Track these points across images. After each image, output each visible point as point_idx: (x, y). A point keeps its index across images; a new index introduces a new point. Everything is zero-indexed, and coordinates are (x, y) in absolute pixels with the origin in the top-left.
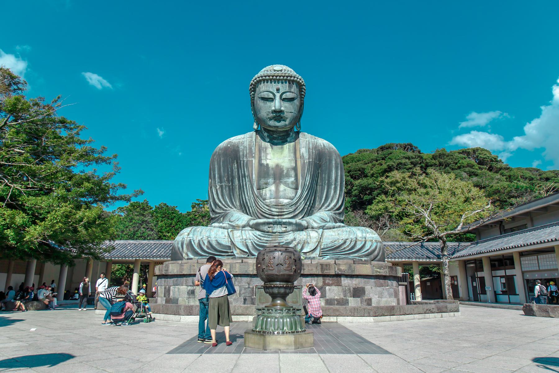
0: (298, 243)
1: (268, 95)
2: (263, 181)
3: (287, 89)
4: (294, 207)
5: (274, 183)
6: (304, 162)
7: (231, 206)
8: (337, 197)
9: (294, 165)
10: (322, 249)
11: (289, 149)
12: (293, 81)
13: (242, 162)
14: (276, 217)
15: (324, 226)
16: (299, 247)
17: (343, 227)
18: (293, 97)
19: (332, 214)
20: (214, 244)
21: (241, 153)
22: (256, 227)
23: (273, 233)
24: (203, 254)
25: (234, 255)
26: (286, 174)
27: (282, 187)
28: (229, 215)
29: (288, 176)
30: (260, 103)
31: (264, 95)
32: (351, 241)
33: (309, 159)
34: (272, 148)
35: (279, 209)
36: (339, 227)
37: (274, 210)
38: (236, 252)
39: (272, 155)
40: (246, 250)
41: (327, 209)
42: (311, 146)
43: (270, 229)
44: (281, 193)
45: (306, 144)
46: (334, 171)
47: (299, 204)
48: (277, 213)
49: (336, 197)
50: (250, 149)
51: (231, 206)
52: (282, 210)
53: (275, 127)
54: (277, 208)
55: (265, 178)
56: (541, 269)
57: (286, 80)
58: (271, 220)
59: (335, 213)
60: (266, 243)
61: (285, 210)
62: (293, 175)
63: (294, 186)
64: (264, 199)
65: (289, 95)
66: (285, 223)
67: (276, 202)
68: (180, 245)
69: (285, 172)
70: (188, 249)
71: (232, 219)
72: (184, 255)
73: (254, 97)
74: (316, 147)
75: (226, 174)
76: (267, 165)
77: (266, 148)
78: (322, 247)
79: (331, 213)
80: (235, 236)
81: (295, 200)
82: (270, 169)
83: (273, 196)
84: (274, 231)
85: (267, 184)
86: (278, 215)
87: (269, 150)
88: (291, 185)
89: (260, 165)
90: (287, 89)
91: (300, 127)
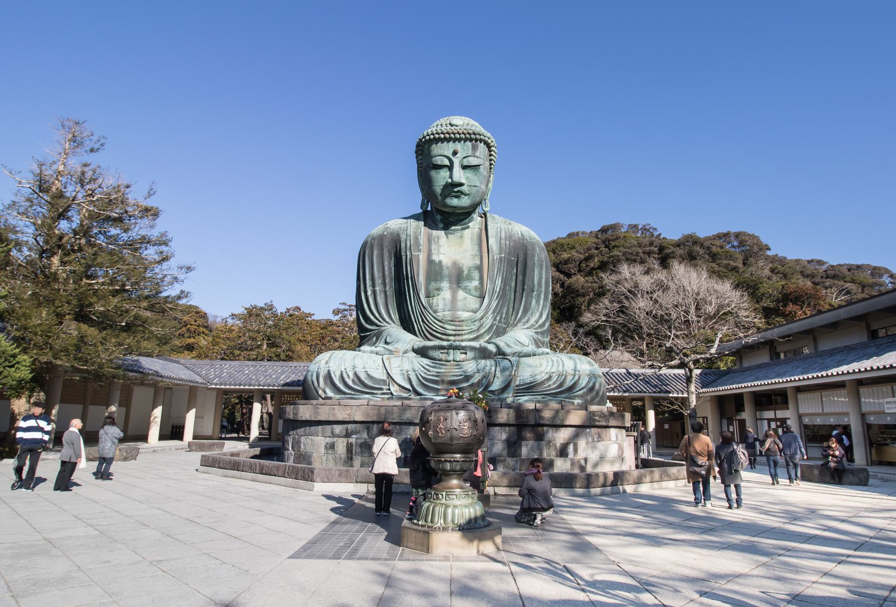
1: (442, 161)
2: (433, 285)
3: (470, 153)
4: (477, 324)
5: (450, 288)
6: (493, 259)
7: (387, 319)
9: (479, 263)
10: (517, 386)
12: (481, 141)
13: (404, 258)
14: (452, 338)
19: (533, 334)
20: (363, 377)
21: (403, 245)
22: (422, 352)
23: (447, 361)
24: (347, 391)
25: (392, 394)
27: (461, 294)
28: (385, 334)
29: (470, 278)
30: (433, 173)
33: (500, 253)
36: (543, 354)
38: (394, 389)
40: (409, 387)
43: (443, 357)
45: (497, 232)
48: (454, 333)
49: (540, 311)
50: (416, 238)
51: (387, 319)
53: (452, 207)
55: (436, 280)
56: (825, 411)
58: (445, 343)
60: (437, 376)
61: (465, 328)
62: (477, 278)
63: (477, 294)
64: (435, 312)
65: (473, 161)
66: (463, 348)
67: (452, 315)
68: (315, 379)
69: (466, 272)
70: (325, 383)
71: (388, 340)
72: (320, 392)
74: (510, 237)
75: (381, 274)
76: (440, 262)
78: (517, 383)
79: (531, 332)
80: (393, 366)
81: (479, 314)
83: (448, 308)
85: (439, 289)
86: (455, 335)
89: (430, 262)
90: (470, 153)
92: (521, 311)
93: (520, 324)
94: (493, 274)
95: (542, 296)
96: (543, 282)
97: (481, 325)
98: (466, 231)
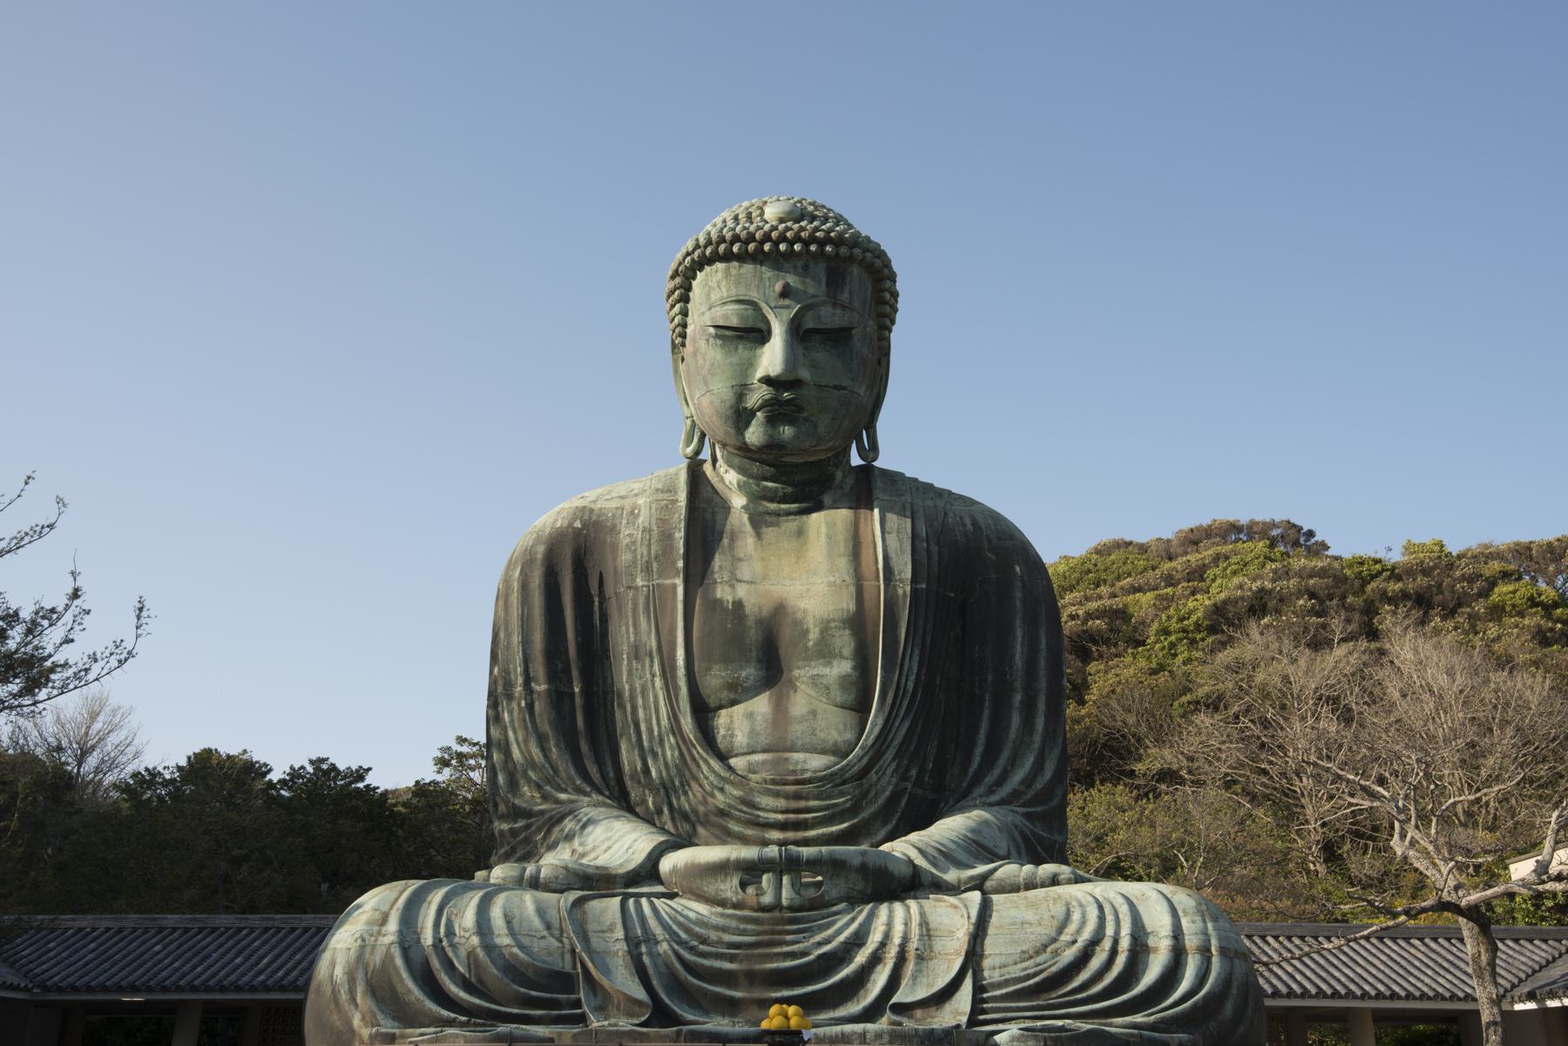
0: (876, 959)
8: (1036, 745)
9: (852, 607)
11: (829, 537)
15: (985, 877)
16: (880, 978)
17: (1069, 882)
18: (845, 324)
19: (1019, 820)
25: (582, 1019)
26: (817, 644)
27: (799, 704)
29: (825, 652)
31: (726, 317)
32: (1114, 952)
34: (758, 535)
35: (787, 797)
36: (1054, 881)
37: (765, 801)
39: (758, 567)
41: (994, 798)
42: (922, 530)
44: (797, 731)
46: (1019, 633)
47: (873, 776)
48: (780, 817)
50: (666, 537)
52: (802, 804)
54: (777, 795)
55: (726, 660)
57: (814, 255)
59: (1025, 815)
60: (731, 958)
61: (812, 803)
63: (850, 698)
65: (830, 317)
68: (339, 972)
73: (684, 325)
76: (738, 605)
77: (734, 537)
79: (1012, 816)
82: (751, 622)
83: (764, 740)
84: (767, 899)
86: (783, 826)
87: (748, 543)
88: (838, 695)
91: (874, 447)
92: (979, 750)
93: (979, 790)
94: (897, 641)
95: (1041, 706)
96: (1042, 664)
97: (864, 795)
98: (814, 515)
